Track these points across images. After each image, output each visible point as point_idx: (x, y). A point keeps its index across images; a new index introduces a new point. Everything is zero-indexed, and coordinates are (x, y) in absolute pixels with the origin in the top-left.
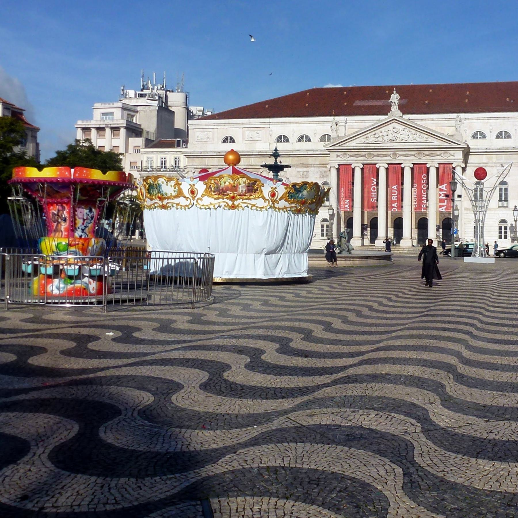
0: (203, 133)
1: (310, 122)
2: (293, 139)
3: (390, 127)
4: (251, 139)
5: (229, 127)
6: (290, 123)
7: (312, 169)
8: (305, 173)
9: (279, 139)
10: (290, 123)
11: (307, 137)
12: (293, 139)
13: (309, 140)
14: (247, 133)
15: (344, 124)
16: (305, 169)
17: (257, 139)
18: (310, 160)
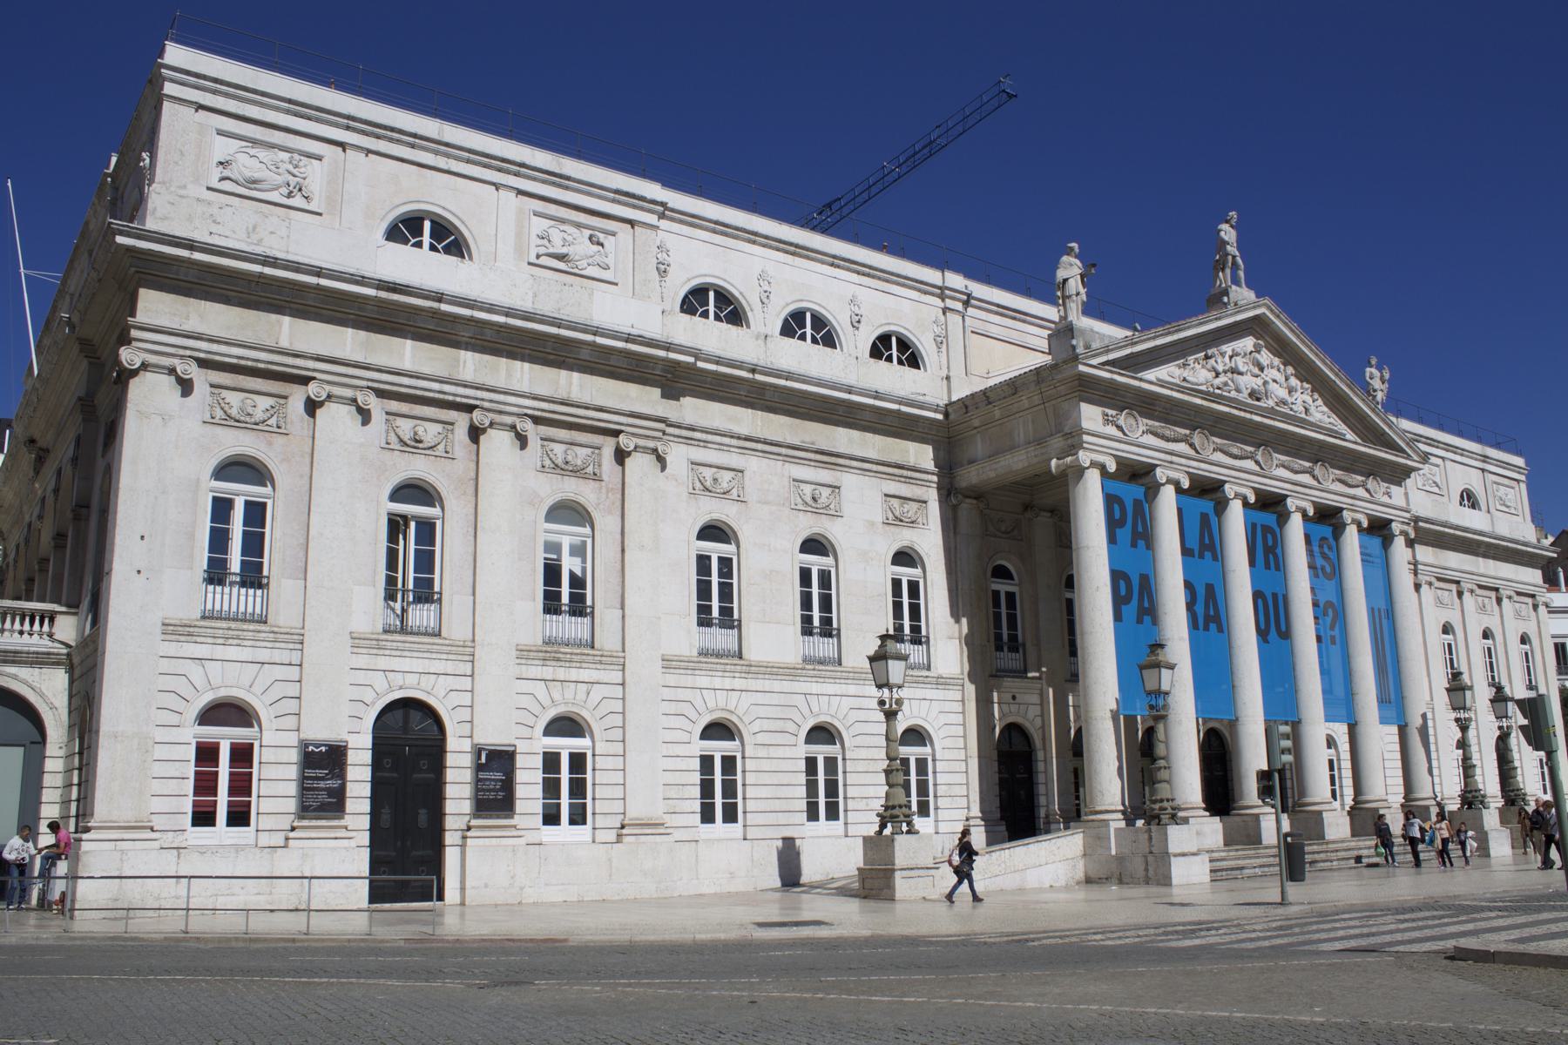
0: (262, 154)
1: (836, 261)
2: (766, 318)
3: (1248, 343)
4: (561, 266)
5: (441, 162)
6: (753, 237)
7: (850, 482)
8: (826, 492)
9: (694, 301)
10: (753, 237)
11: (819, 322)
12: (766, 318)
13: (829, 341)
14: (540, 225)
15: (959, 306)
16: (825, 475)
17: (590, 271)
18: (844, 439)
